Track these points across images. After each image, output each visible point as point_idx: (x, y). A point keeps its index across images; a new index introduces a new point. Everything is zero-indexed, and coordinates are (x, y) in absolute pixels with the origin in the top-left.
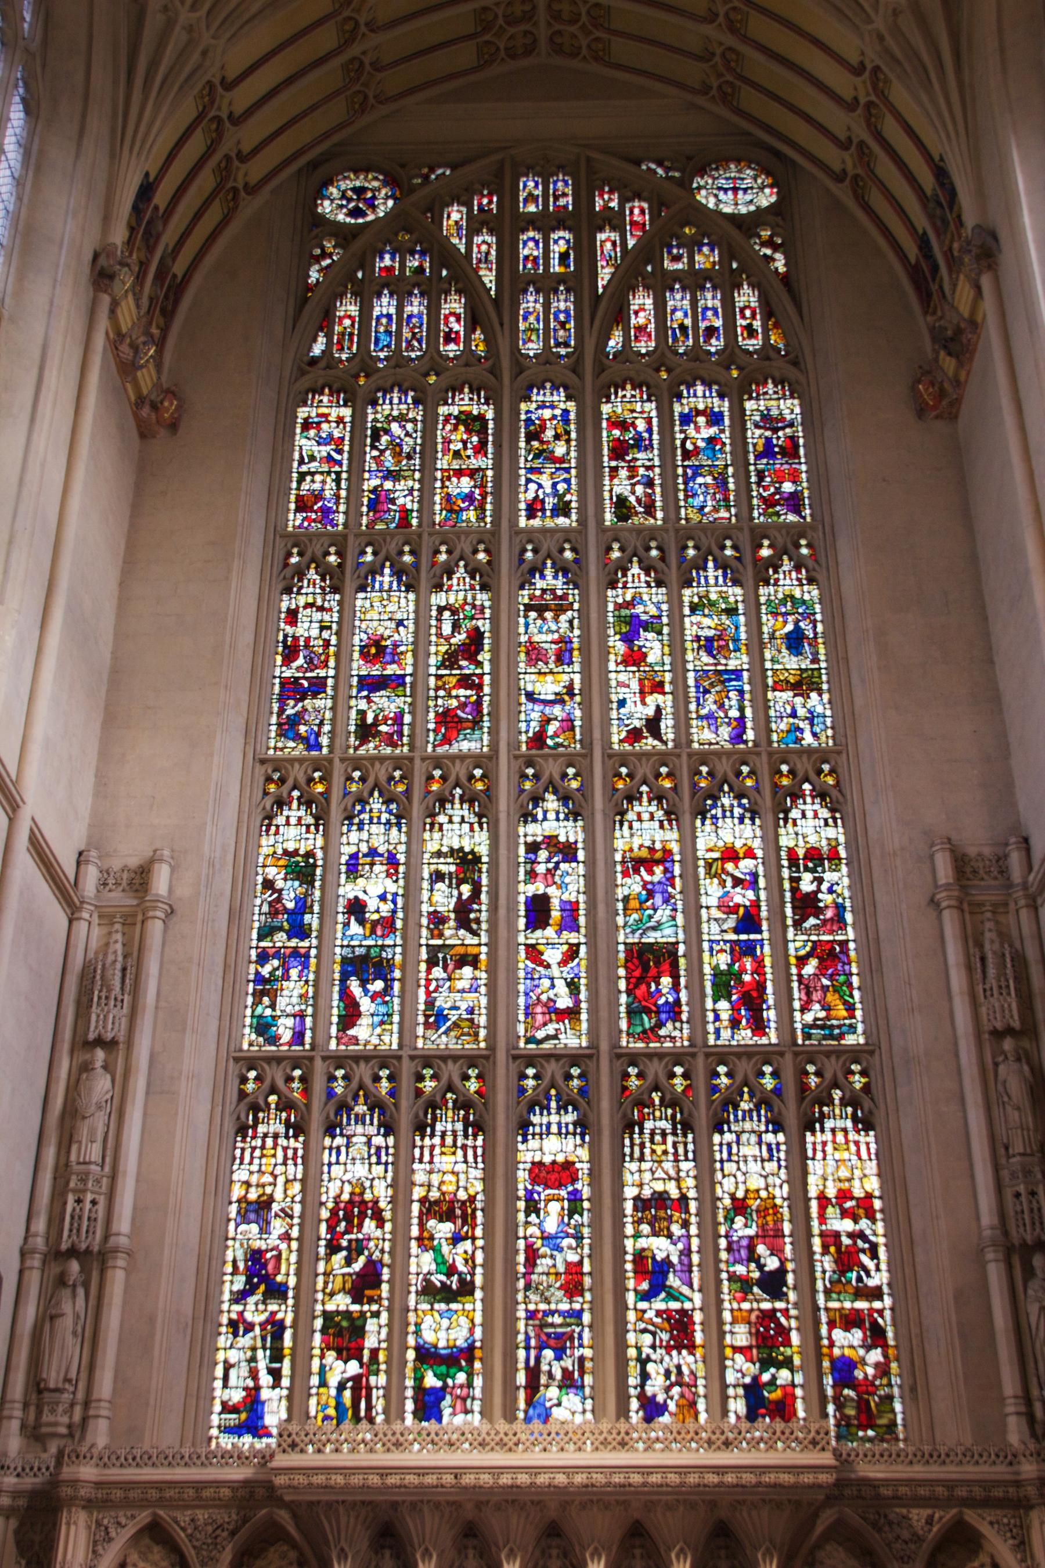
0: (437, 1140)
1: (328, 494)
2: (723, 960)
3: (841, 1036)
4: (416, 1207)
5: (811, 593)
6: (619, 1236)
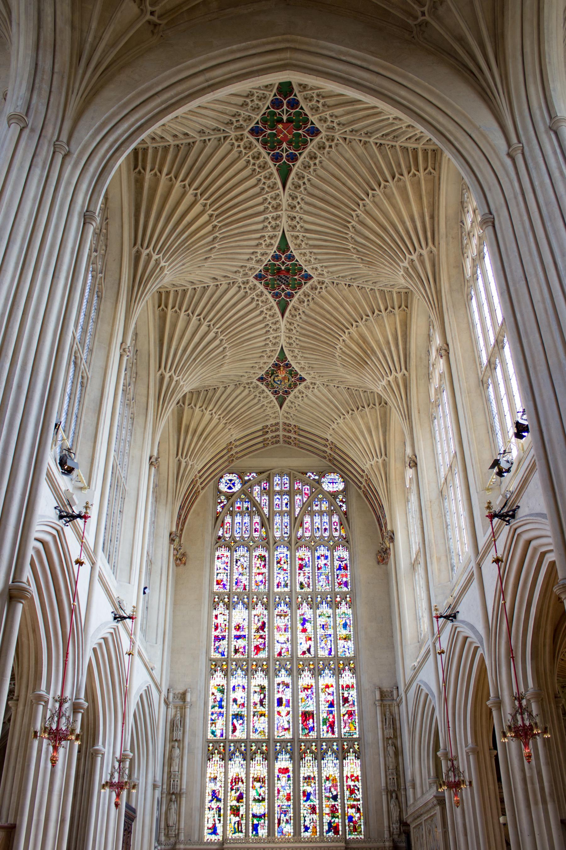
0: (256, 762)
1: (225, 580)
2: (325, 715)
3: (353, 735)
4: (251, 780)
5: (350, 611)
6: (299, 786)
